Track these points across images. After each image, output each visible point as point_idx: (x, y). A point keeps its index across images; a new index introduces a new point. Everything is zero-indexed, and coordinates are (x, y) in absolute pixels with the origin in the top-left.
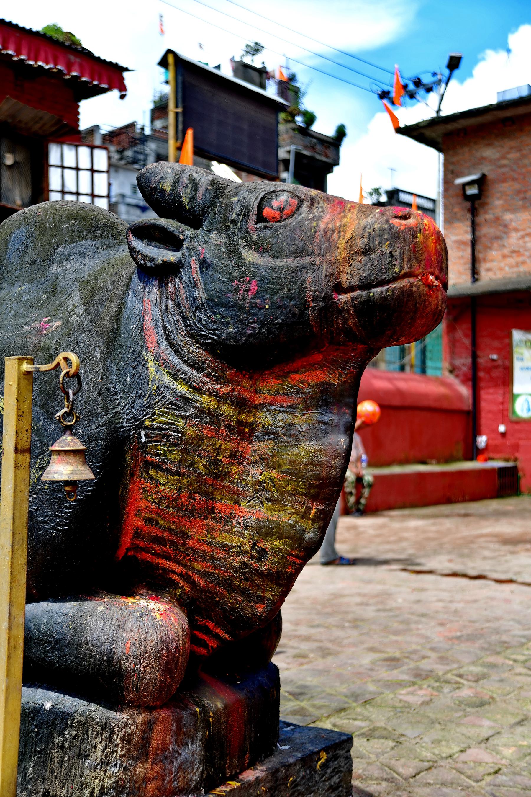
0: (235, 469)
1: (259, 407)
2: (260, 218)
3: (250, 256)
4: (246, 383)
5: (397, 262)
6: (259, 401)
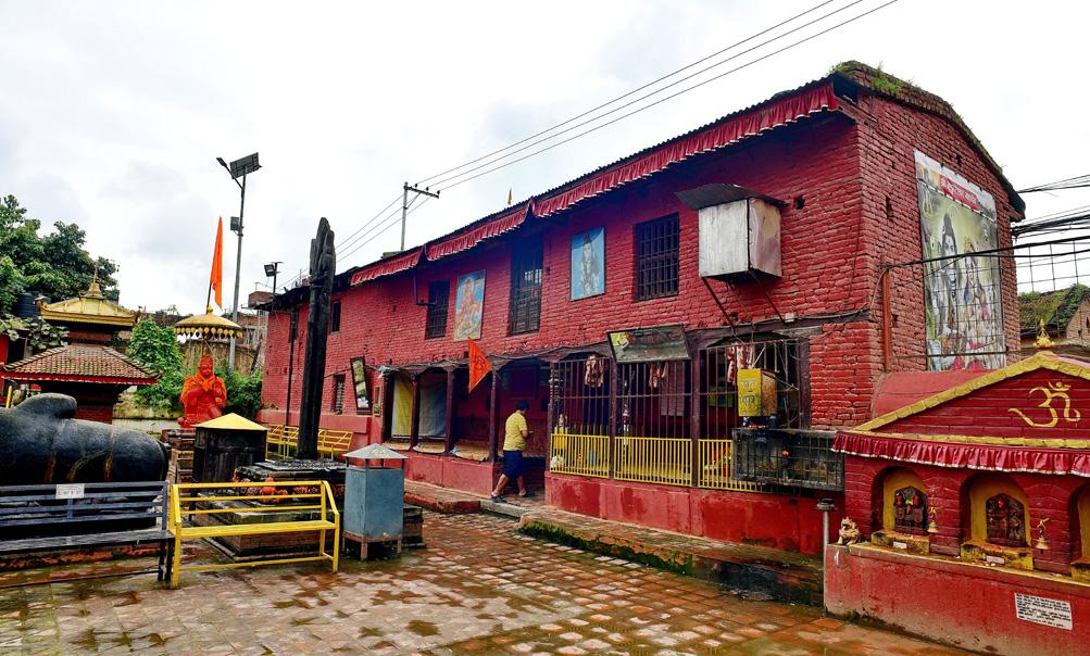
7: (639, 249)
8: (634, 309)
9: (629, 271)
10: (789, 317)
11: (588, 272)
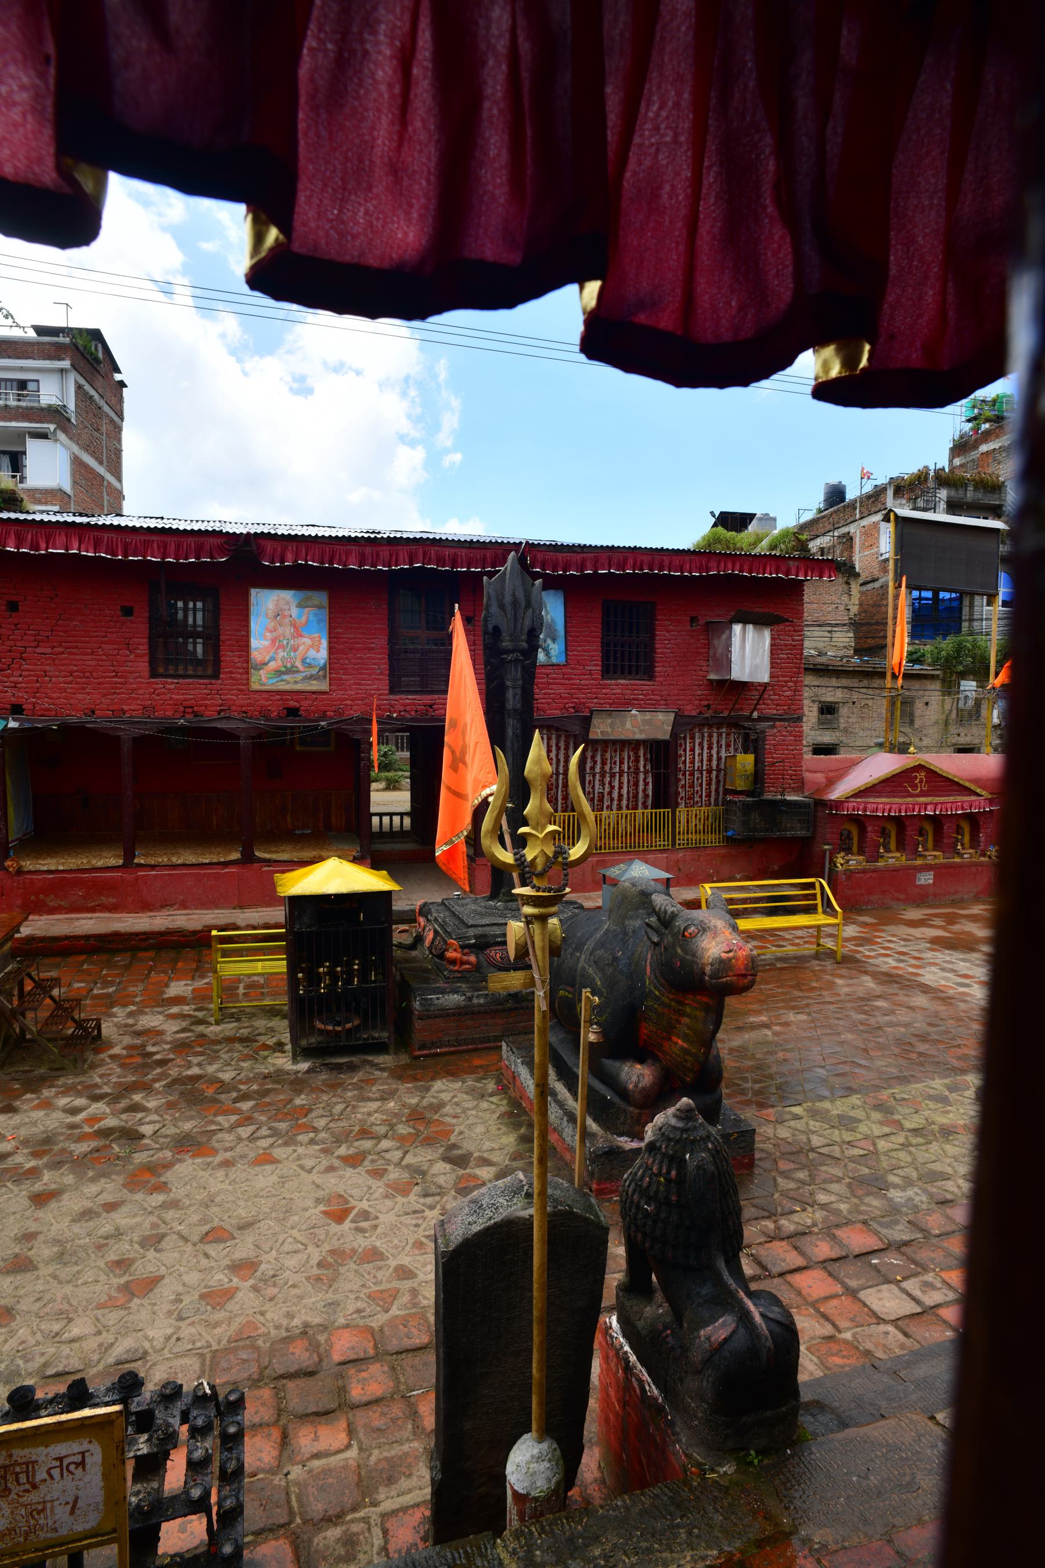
2: (684, 935)
3: (679, 951)
7: (606, 627)
8: (606, 686)
10: (755, 715)
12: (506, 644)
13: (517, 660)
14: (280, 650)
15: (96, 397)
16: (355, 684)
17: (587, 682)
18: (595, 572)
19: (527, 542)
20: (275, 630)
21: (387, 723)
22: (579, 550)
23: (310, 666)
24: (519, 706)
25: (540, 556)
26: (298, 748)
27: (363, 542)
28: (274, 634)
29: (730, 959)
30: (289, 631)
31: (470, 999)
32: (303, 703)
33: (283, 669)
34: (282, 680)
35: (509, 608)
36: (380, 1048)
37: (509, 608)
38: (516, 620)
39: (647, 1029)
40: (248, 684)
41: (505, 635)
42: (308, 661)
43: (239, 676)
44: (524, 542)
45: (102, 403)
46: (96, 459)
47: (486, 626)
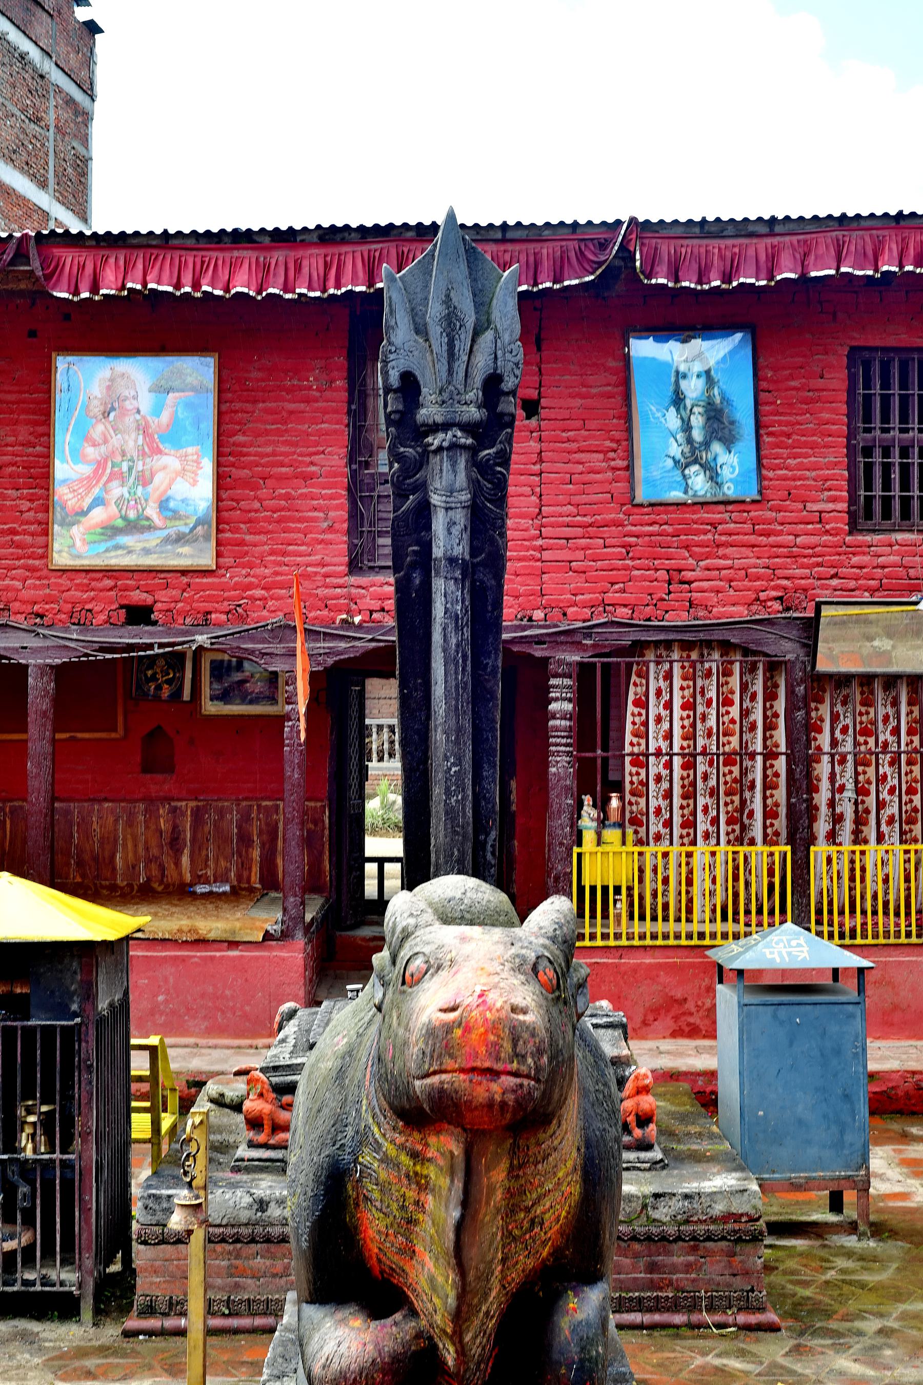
0: (420, 1216)
1: (429, 1160)
4: (417, 1136)
5: (427, 1060)
6: (430, 1155)
7: (861, 411)
9: (836, 455)
11: (698, 435)
12: (429, 411)
13: (454, 446)
14: (115, 484)
15: (34, 54)
16: (272, 553)
17: (813, 539)
18: (804, 277)
19: (633, 221)
20: (106, 441)
21: (342, 637)
22: (764, 230)
23: (176, 515)
24: (461, 550)
25: (666, 249)
26: (211, 708)
27: (267, 240)
28: (103, 449)
29: (448, 1028)
30: (133, 442)
31: (262, 1205)
32: (162, 595)
33: (120, 523)
34: (117, 547)
35: (435, 331)
36: (61, 1307)
37: (435, 331)
38: (452, 356)
39: (375, 1225)
40: (45, 556)
41: (428, 394)
42: (172, 505)
43: (29, 539)
44: (625, 218)
45: (47, 67)
46: (33, 177)
47: (386, 374)
